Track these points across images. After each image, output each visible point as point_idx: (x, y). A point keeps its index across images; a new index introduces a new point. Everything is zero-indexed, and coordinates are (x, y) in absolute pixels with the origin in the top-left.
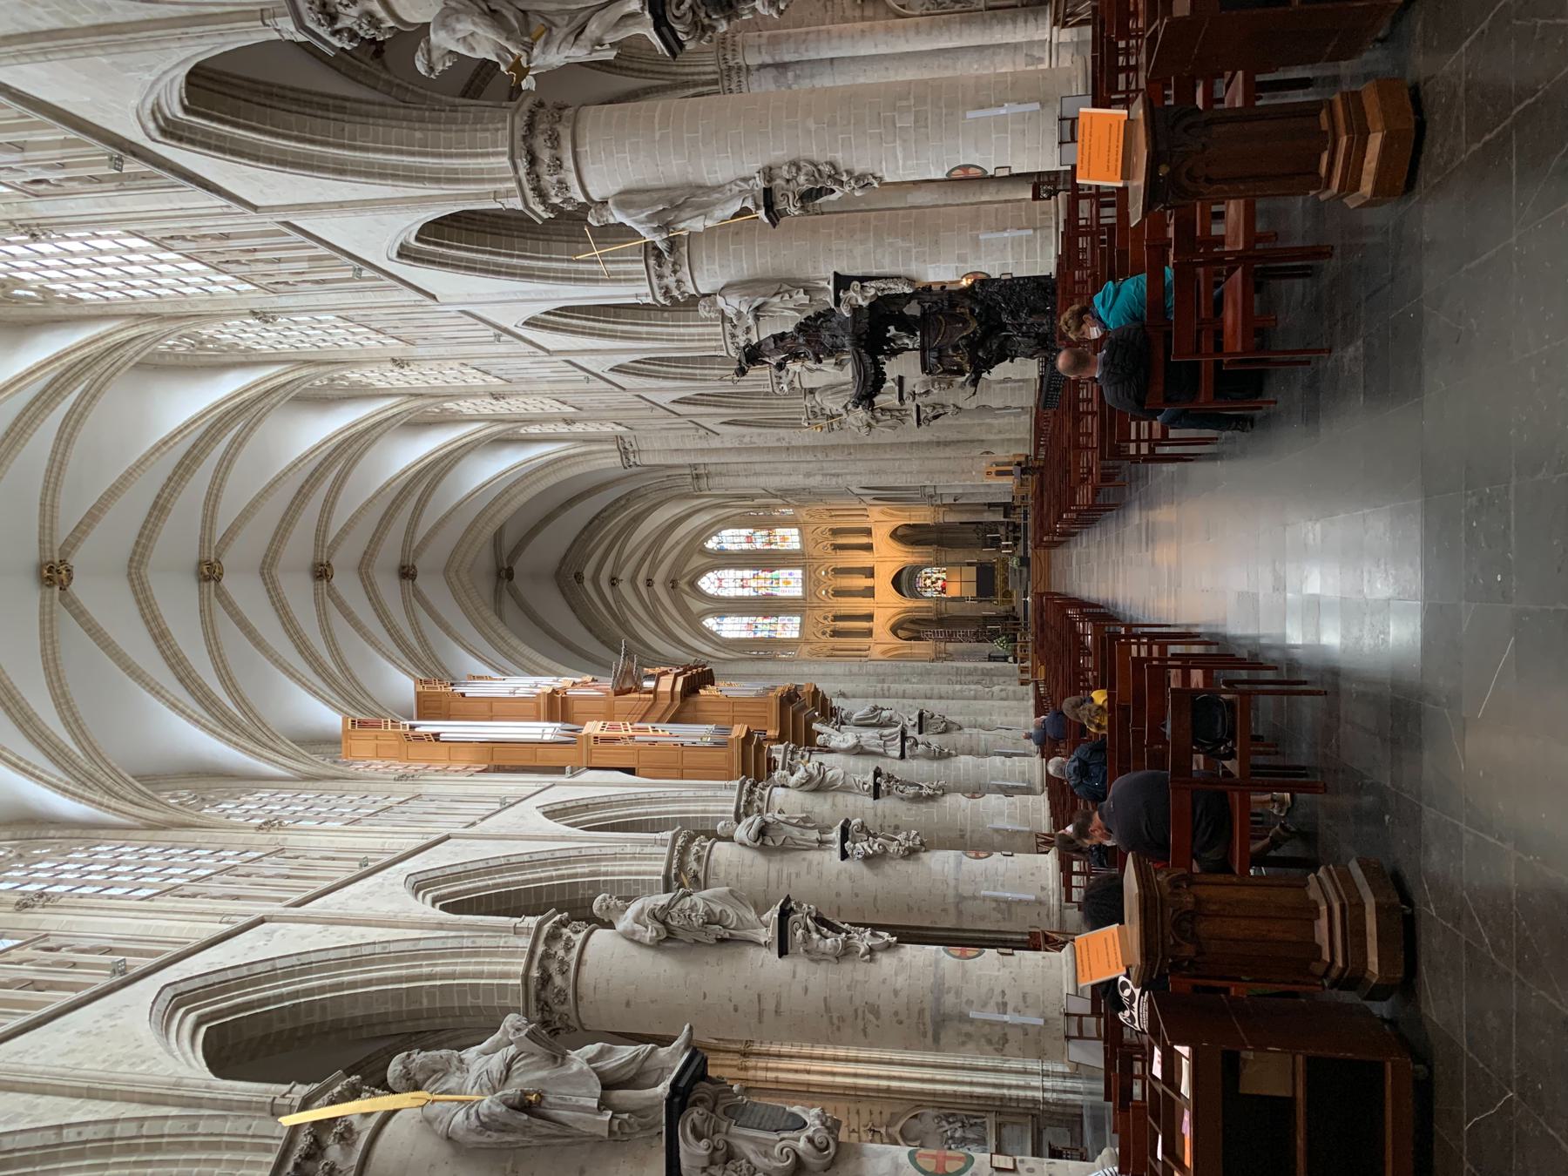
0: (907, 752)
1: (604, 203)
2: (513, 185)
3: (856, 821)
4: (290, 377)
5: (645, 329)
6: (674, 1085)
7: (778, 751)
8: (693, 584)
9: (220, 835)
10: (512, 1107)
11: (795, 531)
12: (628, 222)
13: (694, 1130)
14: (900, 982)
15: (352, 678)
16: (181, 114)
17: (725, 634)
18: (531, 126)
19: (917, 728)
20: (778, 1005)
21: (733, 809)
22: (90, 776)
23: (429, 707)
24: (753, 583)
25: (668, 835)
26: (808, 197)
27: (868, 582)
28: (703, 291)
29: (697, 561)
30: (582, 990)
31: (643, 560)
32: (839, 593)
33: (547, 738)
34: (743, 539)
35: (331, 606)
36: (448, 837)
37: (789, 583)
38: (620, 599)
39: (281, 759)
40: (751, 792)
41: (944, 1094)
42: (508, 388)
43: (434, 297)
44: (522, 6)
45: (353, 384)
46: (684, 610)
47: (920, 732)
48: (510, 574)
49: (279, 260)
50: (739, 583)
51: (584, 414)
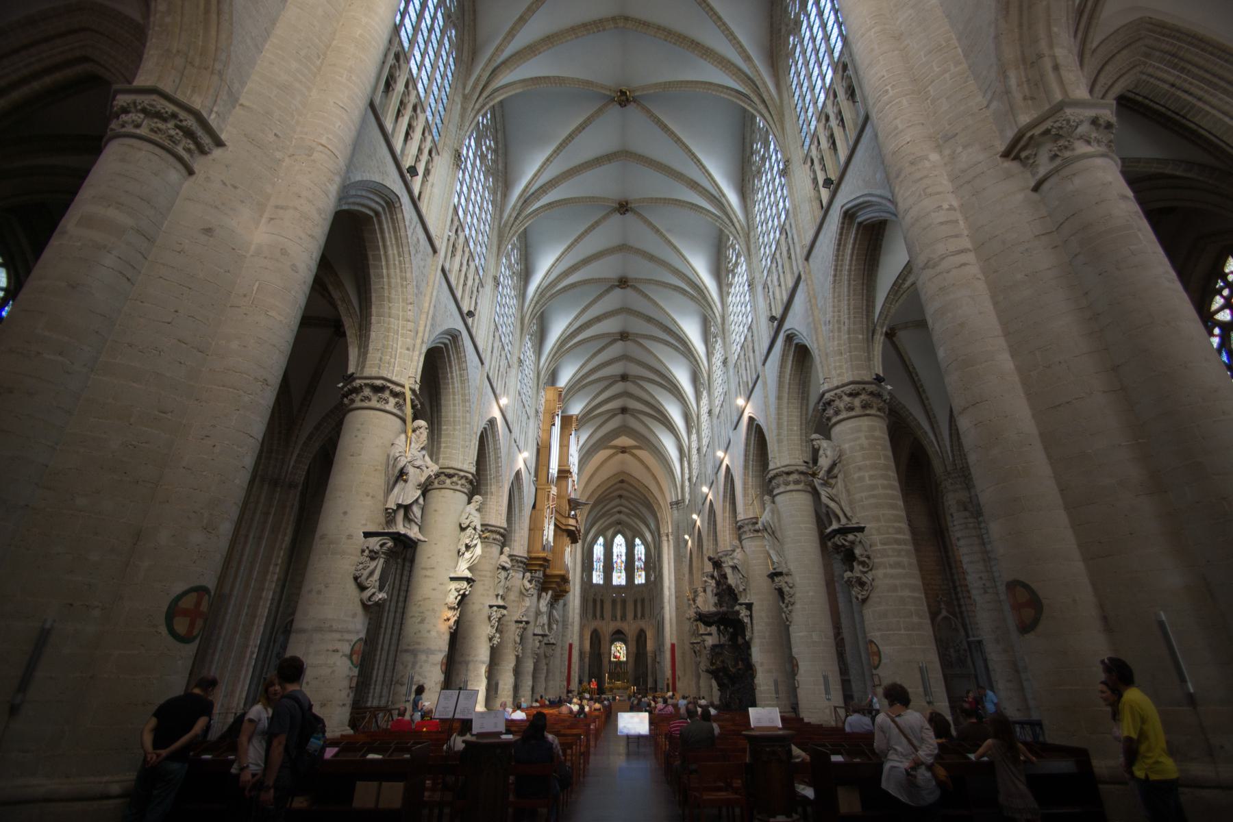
0: (536, 637)
1: (773, 502)
2: (778, 465)
3: (505, 612)
4: (703, 369)
5: (727, 515)
6: (405, 535)
9: (517, 344)
10: (402, 469)
11: (643, 581)
12: (766, 512)
13: (385, 544)
14: (433, 634)
15: (579, 390)
16: (795, 342)
17: (595, 547)
18: (802, 473)
20: (429, 577)
21: (515, 553)
22: (543, 296)
23: (566, 421)
24: (619, 561)
25: (505, 525)
26: (780, 592)
27: (619, 618)
28: (743, 542)
29: (629, 534)
30: (443, 490)
31: (630, 509)
32: (614, 602)
33: (551, 471)
35: (611, 381)
36: (510, 431)
38: (612, 499)
39: (547, 364)
40: (521, 562)
41: (375, 655)
42: (702, 455)
43: (735, 428)
44: (839, 476)
45: (702, 393)
47: (546, 644)
48: (623, 452)
49: (746, 370)
51: (693, 486)
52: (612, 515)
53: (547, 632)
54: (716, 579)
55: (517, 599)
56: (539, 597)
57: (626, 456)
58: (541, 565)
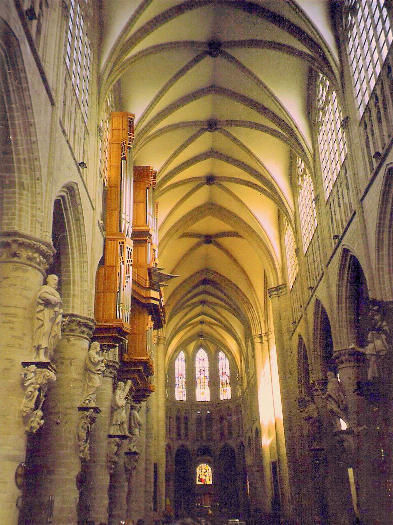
7: (114, 358)
8: (201, 346)
17: (177, 362)
19: (127, 451)
21: (75, 313)
24: (202, 376)
25: (50, 240)
29: (212, 347)
33: (123, 216)
34: (224, 371)
37: (203, 395)
38: (194, 306)
40: (86, 326)
46: (190, 340)
47: (126, 454)
50: (202, 370)
52: (195, 325)
53: (129, 435)
54: (385, 332)
55: (79, 377)
56: (115, 388)
57: (212, 248)
58: (115, 339)
